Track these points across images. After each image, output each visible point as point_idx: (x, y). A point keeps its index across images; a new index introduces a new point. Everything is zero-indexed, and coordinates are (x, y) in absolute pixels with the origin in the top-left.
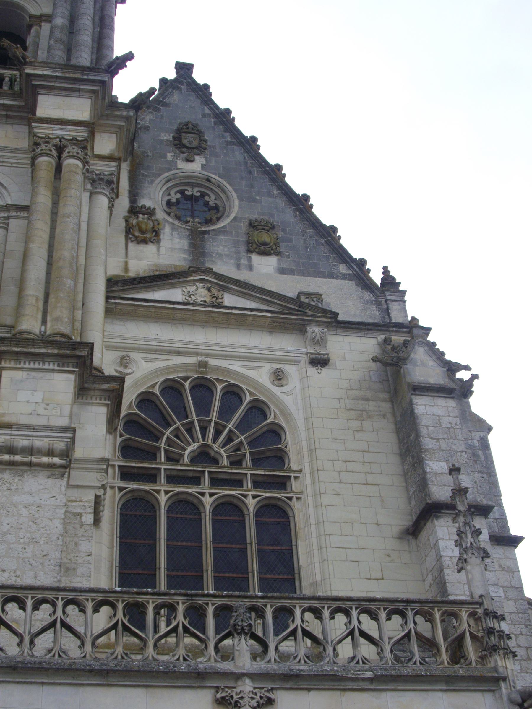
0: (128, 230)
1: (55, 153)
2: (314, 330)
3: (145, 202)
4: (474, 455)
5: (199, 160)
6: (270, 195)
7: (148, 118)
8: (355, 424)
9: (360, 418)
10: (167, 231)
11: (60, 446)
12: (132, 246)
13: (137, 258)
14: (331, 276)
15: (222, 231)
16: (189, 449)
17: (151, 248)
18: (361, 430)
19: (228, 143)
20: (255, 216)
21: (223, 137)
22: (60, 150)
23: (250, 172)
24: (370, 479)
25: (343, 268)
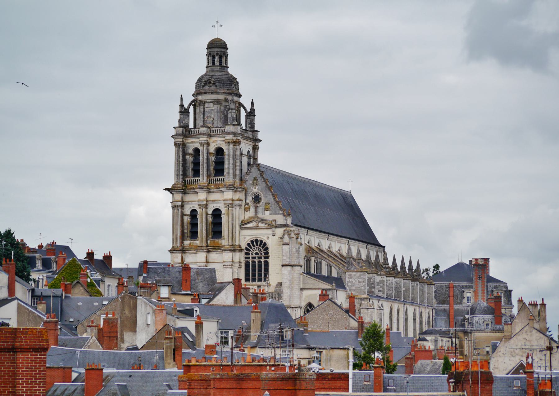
0: (245, 209)
1: (227, 206)
2: (273, 229)
3: (248, 201)
4: (297, 251)
5: (257, 187)
6: (269, 195)
7: (248, 177)
8: (278, 247)
9: (279, 245)
10: (251, 208)
11: (231, 264)
12: (245, 212)
13: (246, 215)
14: (279, 214)
15: (260, 206)
16: (255, 252)
17: (249, 212)
18: (279, 248)
19: (263, 181)
20: (266, 201)
21: (261, 180)
22: (228, 205)
23: (266, 189)
24: (280, 257)
25: (281, 212)
